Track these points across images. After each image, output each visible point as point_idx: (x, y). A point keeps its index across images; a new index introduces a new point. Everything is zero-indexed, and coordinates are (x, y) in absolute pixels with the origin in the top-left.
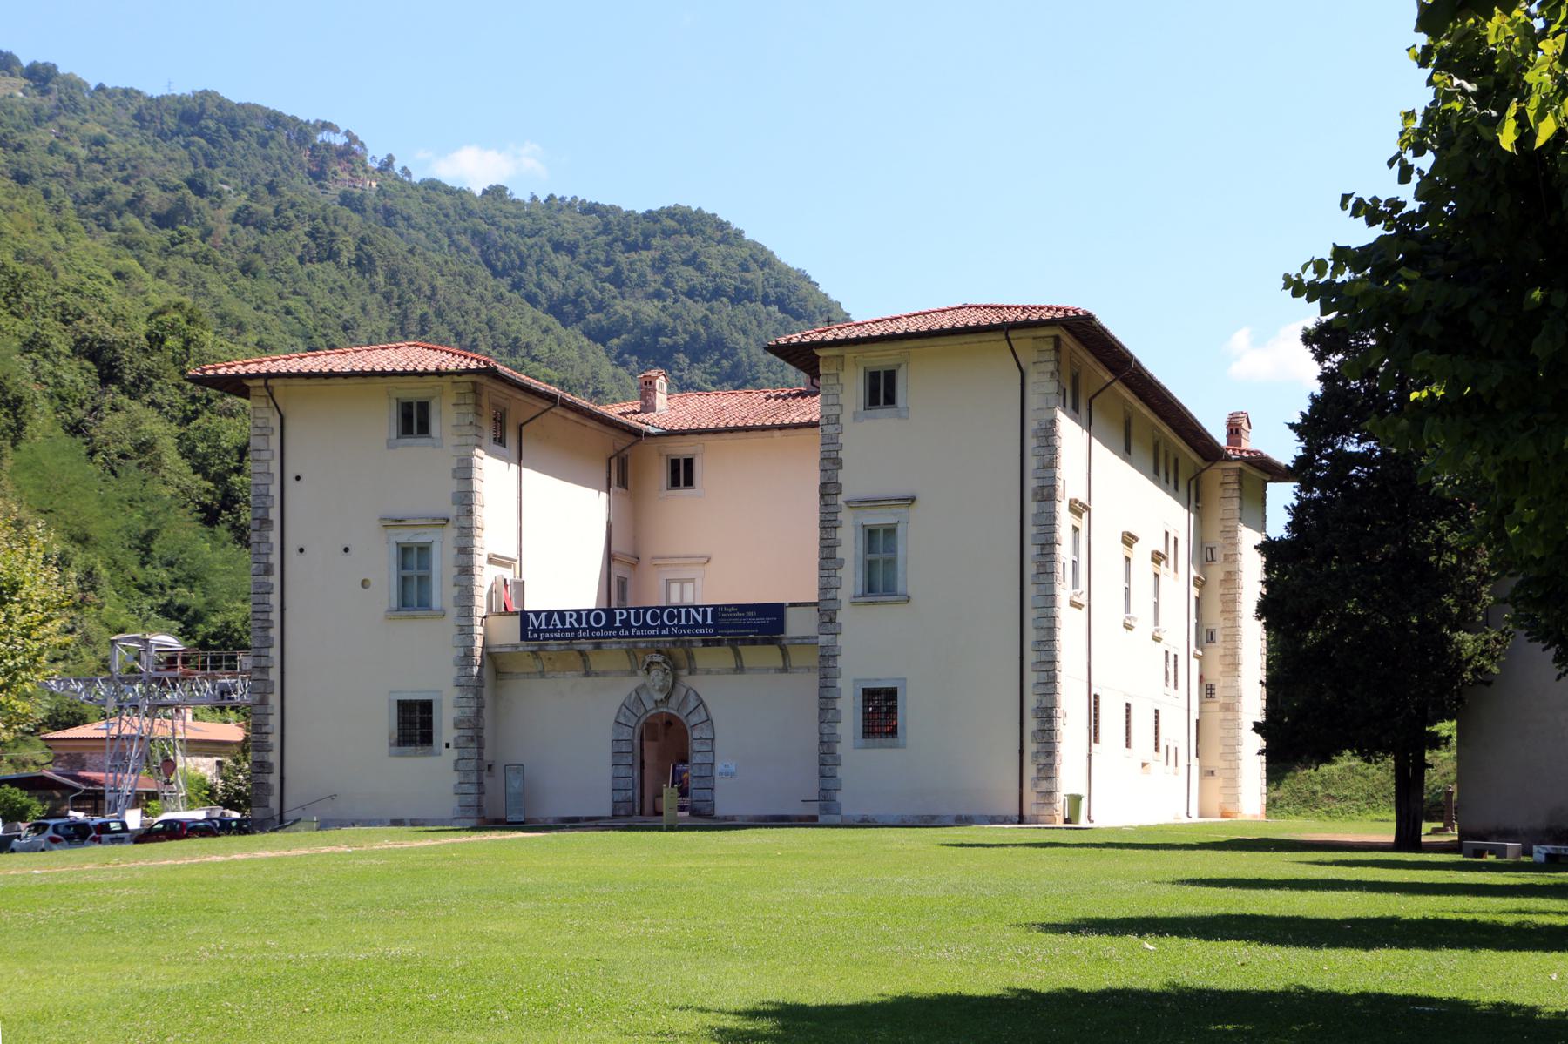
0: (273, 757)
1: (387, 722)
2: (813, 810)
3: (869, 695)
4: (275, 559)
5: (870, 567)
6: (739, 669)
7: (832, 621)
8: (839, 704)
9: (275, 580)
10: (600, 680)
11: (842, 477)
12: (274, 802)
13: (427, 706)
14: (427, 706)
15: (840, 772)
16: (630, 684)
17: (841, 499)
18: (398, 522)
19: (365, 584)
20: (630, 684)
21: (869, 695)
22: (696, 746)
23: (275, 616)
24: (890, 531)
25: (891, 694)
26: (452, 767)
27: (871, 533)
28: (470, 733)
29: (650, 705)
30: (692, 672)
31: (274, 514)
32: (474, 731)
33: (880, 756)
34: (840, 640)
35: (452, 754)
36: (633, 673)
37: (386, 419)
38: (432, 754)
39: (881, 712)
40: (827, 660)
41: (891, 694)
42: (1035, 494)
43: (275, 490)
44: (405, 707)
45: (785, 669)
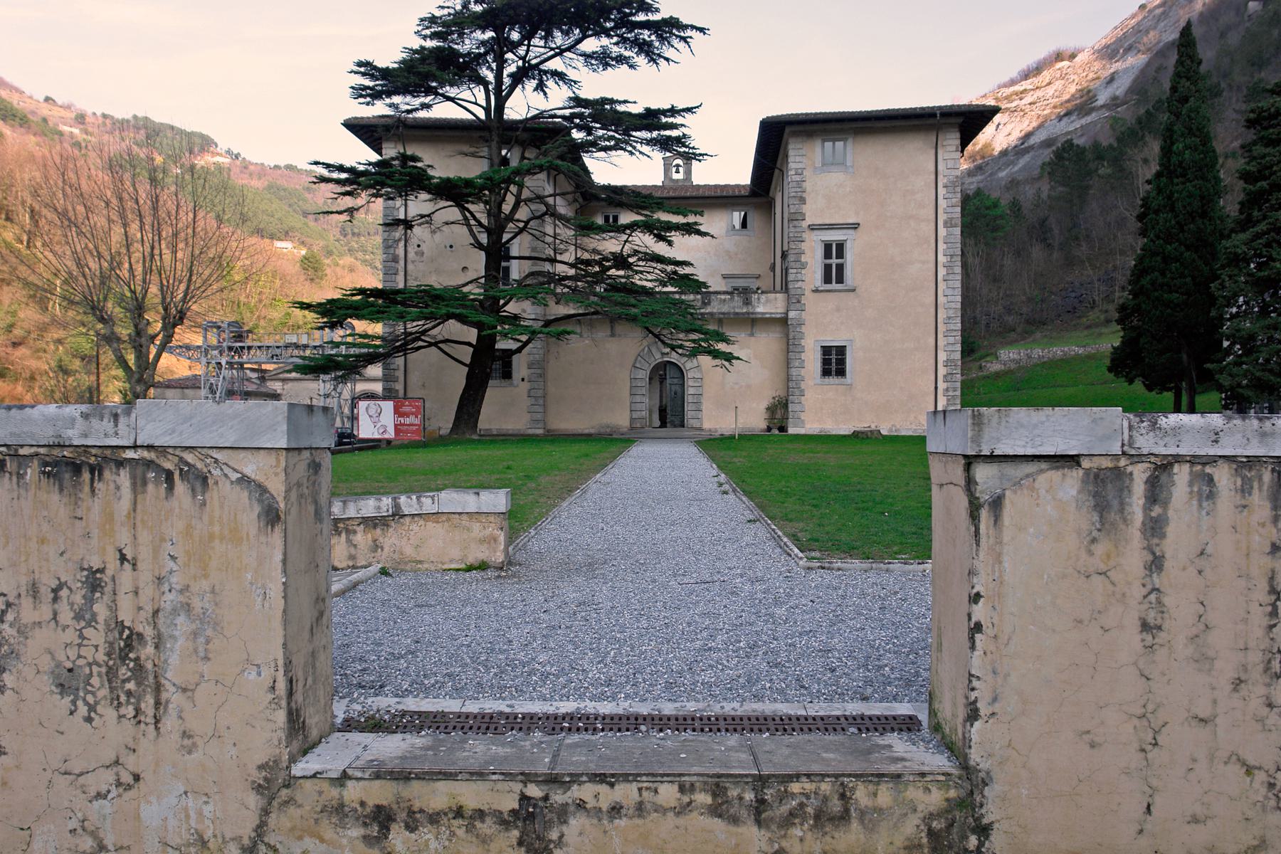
3: (826, 350)
5: (827, 268)
7: (799, 302)
11: (806, 209)
21: (826, 350)
22: (691, 383)
24: (841, 247)
25: (841, 350)
26: (526, 395)
28: (539, 371)
35: (525, 386)
38: (511, 385)
39: (834, 362)
41: (841, 350)
42: (945, 223)
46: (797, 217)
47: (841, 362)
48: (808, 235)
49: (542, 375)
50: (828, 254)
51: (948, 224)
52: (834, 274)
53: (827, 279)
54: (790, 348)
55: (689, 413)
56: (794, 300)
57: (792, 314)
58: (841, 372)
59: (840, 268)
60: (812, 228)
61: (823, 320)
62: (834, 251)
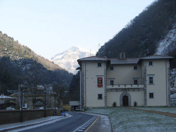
0: (85, 100)
1: (97, 96)
2: (144, 105)
3: (150, 94)
4: (85, 79)
5: (150, 81)
6: (134, 91)
8: (147, 95)
9: (85, 81)
10: (118, 92)
12: (85, 105)
13: (101, 95)
14: (101, 95)
15: (147, 101)
16: (122, 93)
17: (147, 74)
18: (98, 76)
19: (95, 82)
20: (122, 93)
21: (150, 94)
23: (85, 85)
25: (152, 94)
27: (150, 78)
29: (124, 95)
30: (128, 91)
31: (85, 75)
32: (106, 97)
33: (151, 100)
34: (147, 88)
36: (122, 91)
37: (97, 65)
39: (151, 95)
40: (144, 90)
41: (152, 94)
43: (85, 72)
44: (99, 95)
45: (139, 91)
46: (145, 73)
47: (153, 95)
48: (147, 76)
49: (106, 98)
50: (150, 79)
51: (168, 74)
52: (151, 82)
53: (150, 83)
54: (145, 93)
55: (129, 104)
56: (145, 86)
57: (145, 88)
58: (153, 97)
59: (152, 81)
60: (148, 75)
61: (150, 89)
62: (151, 78)
